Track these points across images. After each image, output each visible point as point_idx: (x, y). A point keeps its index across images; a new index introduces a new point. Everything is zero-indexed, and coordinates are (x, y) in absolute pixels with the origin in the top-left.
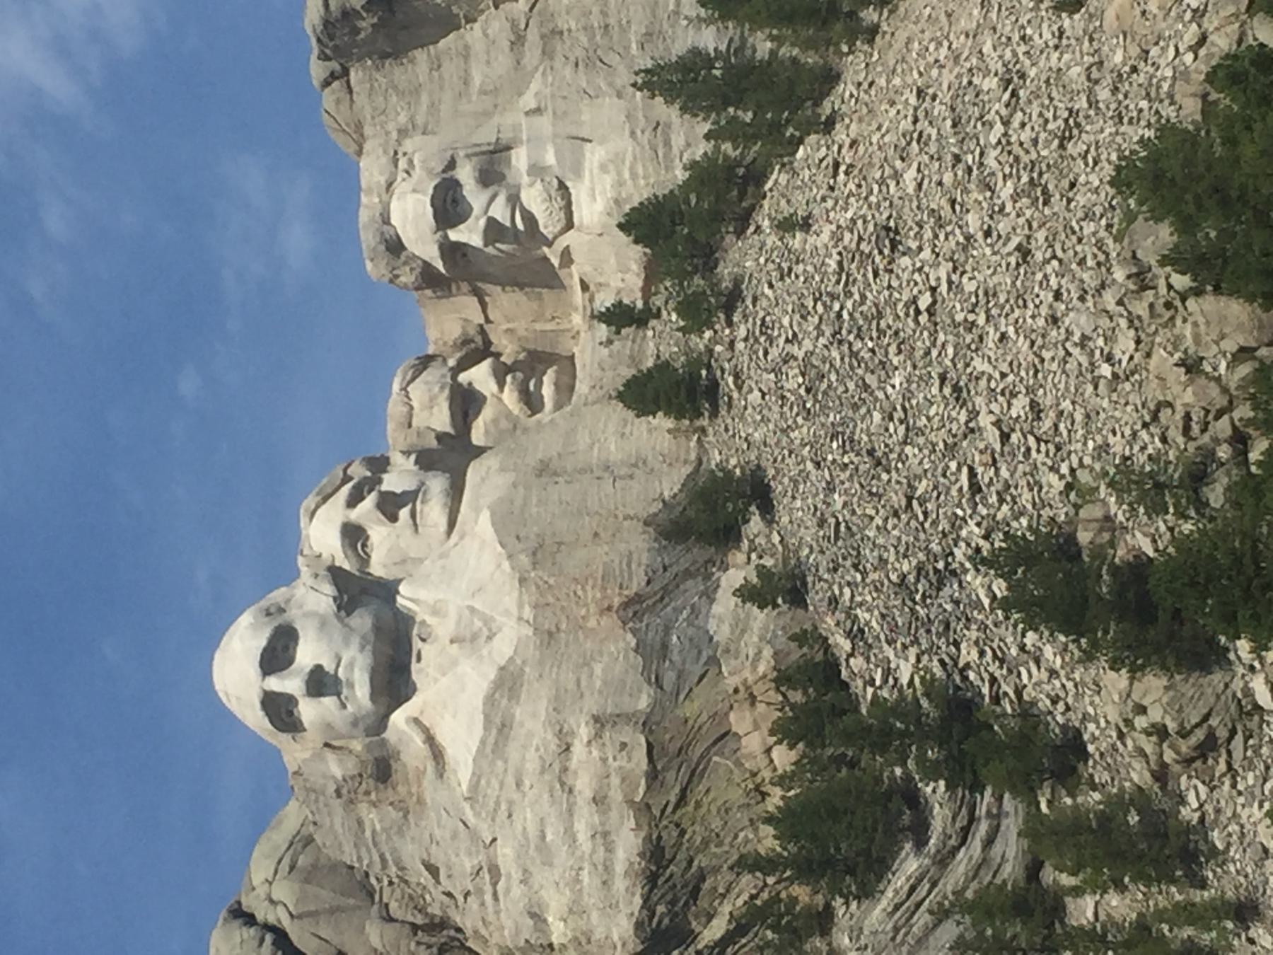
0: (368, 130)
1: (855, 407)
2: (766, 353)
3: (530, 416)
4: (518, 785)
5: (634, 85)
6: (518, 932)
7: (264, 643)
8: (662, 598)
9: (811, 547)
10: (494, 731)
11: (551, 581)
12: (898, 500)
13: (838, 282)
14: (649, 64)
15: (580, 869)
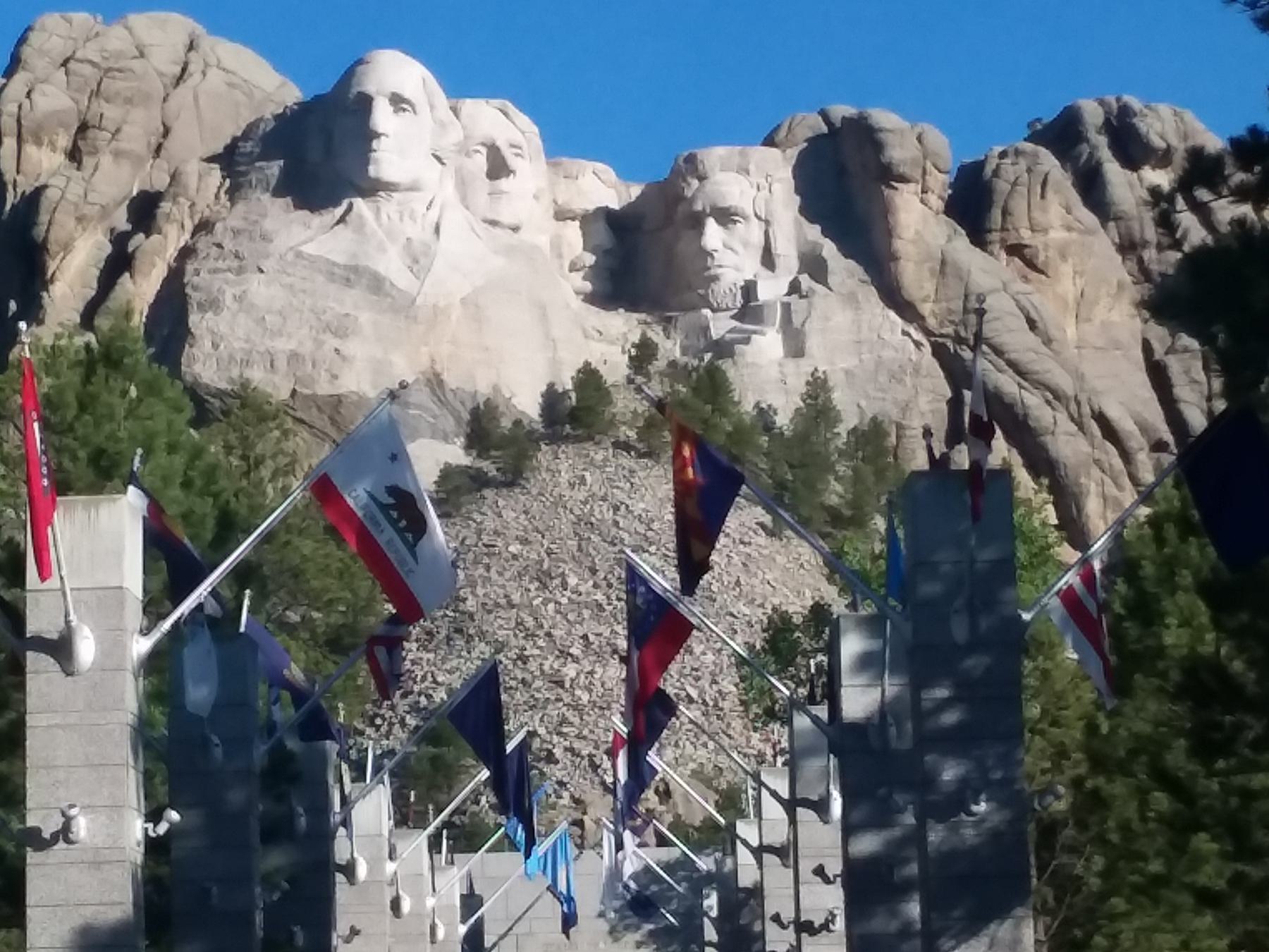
0: (789, 151)
1: (580, 563)
2: (618, 487)
3: (571, 271)
4: (304, 291)
5: (816, 370)
6: (195, 288)
7: (407, 95)
8: (440, 400)
9: (481, 523)
10: (345, 274)
11: (454, 318)
12: (516, 598)
13: (668, 549)
14: (831, 384)
15: (247, 341)
